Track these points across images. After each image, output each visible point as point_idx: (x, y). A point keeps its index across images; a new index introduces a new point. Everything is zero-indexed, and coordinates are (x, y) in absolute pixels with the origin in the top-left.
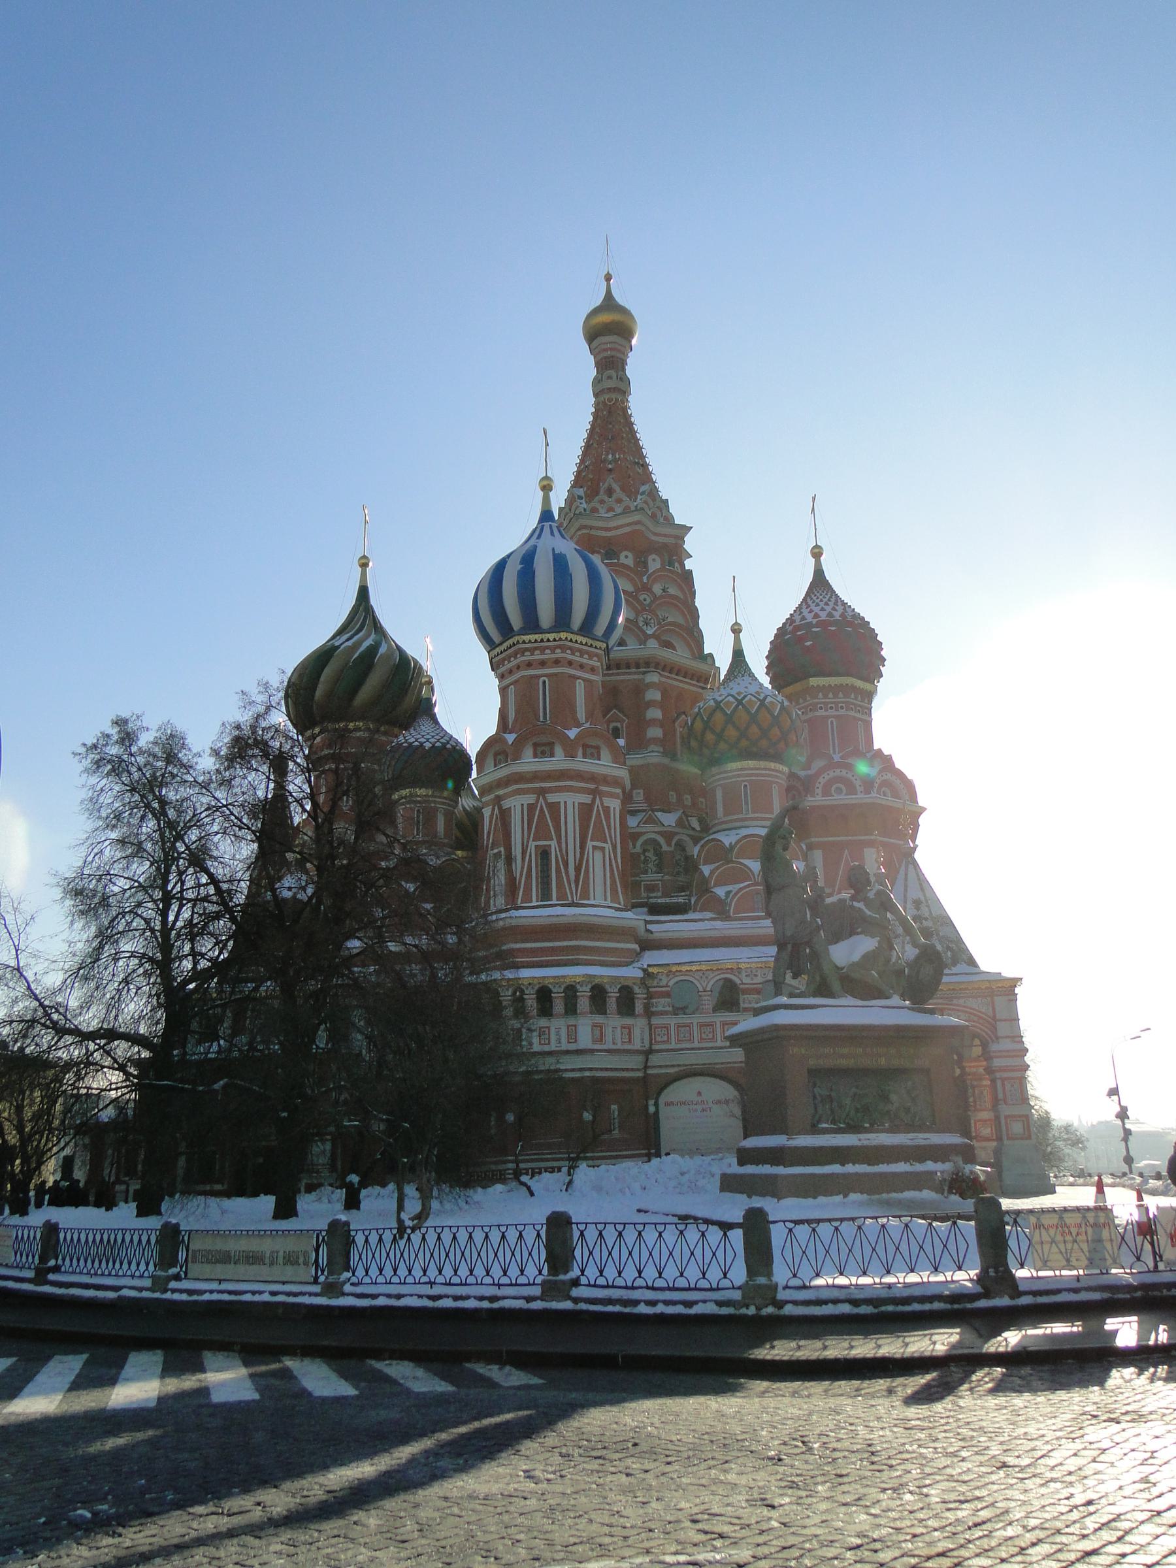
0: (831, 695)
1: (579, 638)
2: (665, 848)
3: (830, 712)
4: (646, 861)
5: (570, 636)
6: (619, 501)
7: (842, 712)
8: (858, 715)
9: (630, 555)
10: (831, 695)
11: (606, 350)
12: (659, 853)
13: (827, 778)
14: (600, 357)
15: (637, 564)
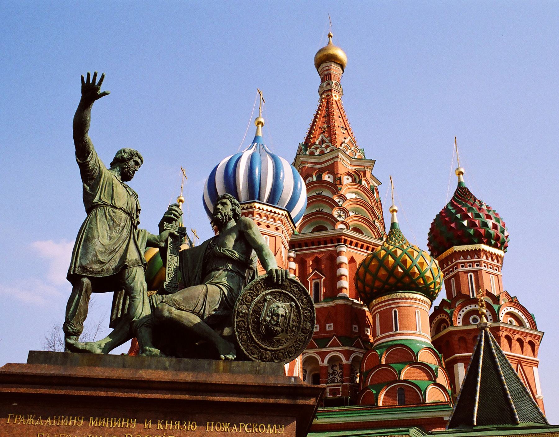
0: (469, 257)
1: (265, 207)
2: (344, 361)
3: (469, 268)
4: (333, 373)
5: (257, 205)
6: (327, 147)
7: (476, 268)
8: (491, 271)
9: (331, 176)
10: (469, 257)
11: (327, 70)
12: (341, 366)
13: (465, 311)
14: (322, 76)
15: (334, 180)
